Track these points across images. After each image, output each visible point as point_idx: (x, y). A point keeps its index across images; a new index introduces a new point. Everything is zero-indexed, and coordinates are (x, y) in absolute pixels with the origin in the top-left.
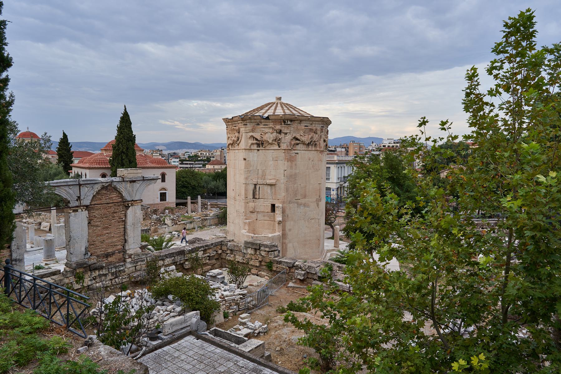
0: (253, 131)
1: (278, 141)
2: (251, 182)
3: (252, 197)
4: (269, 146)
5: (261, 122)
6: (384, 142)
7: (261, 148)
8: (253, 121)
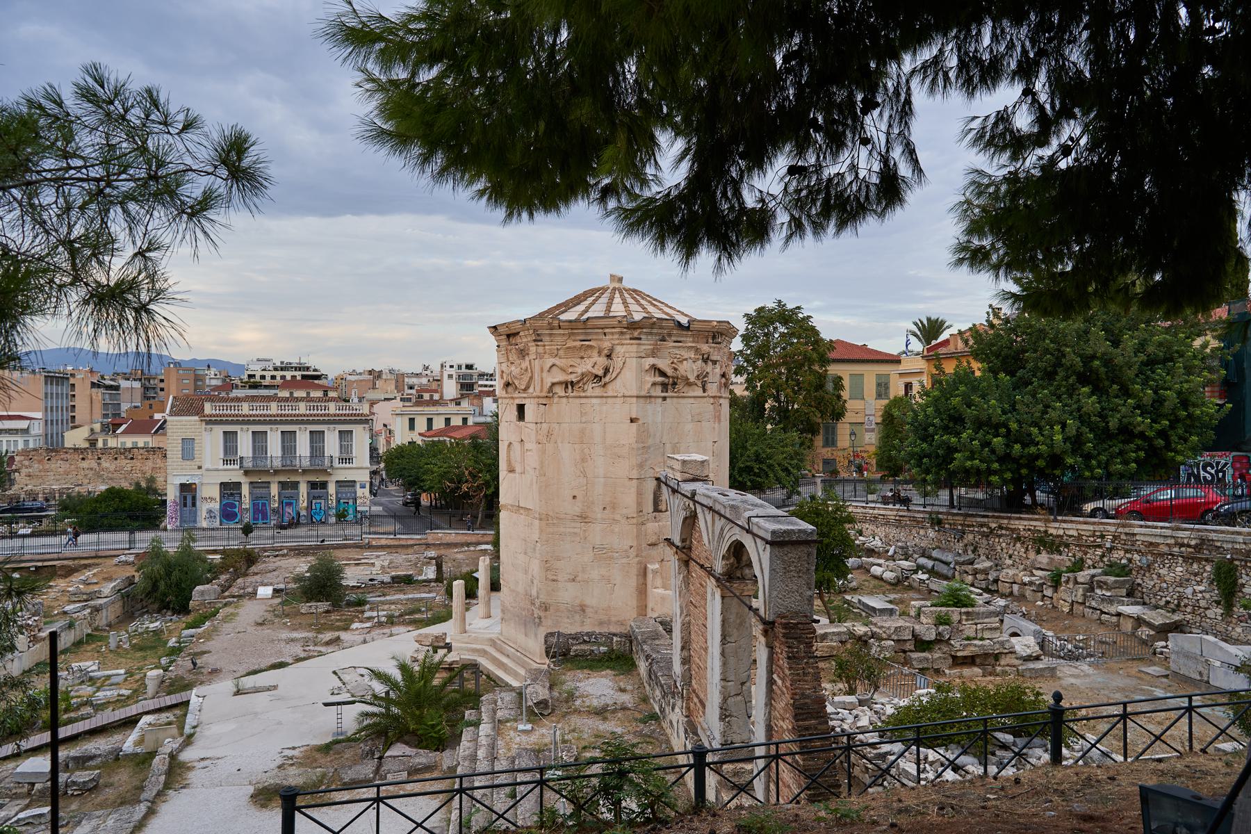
0: (653, 354)
1: (703, 379)
2: (651, 473)
3: (651, 509)
4: (685, 389)
5: (670, 335)
6: (251, 367)
7: (670, 394)
8: (655, 331)
